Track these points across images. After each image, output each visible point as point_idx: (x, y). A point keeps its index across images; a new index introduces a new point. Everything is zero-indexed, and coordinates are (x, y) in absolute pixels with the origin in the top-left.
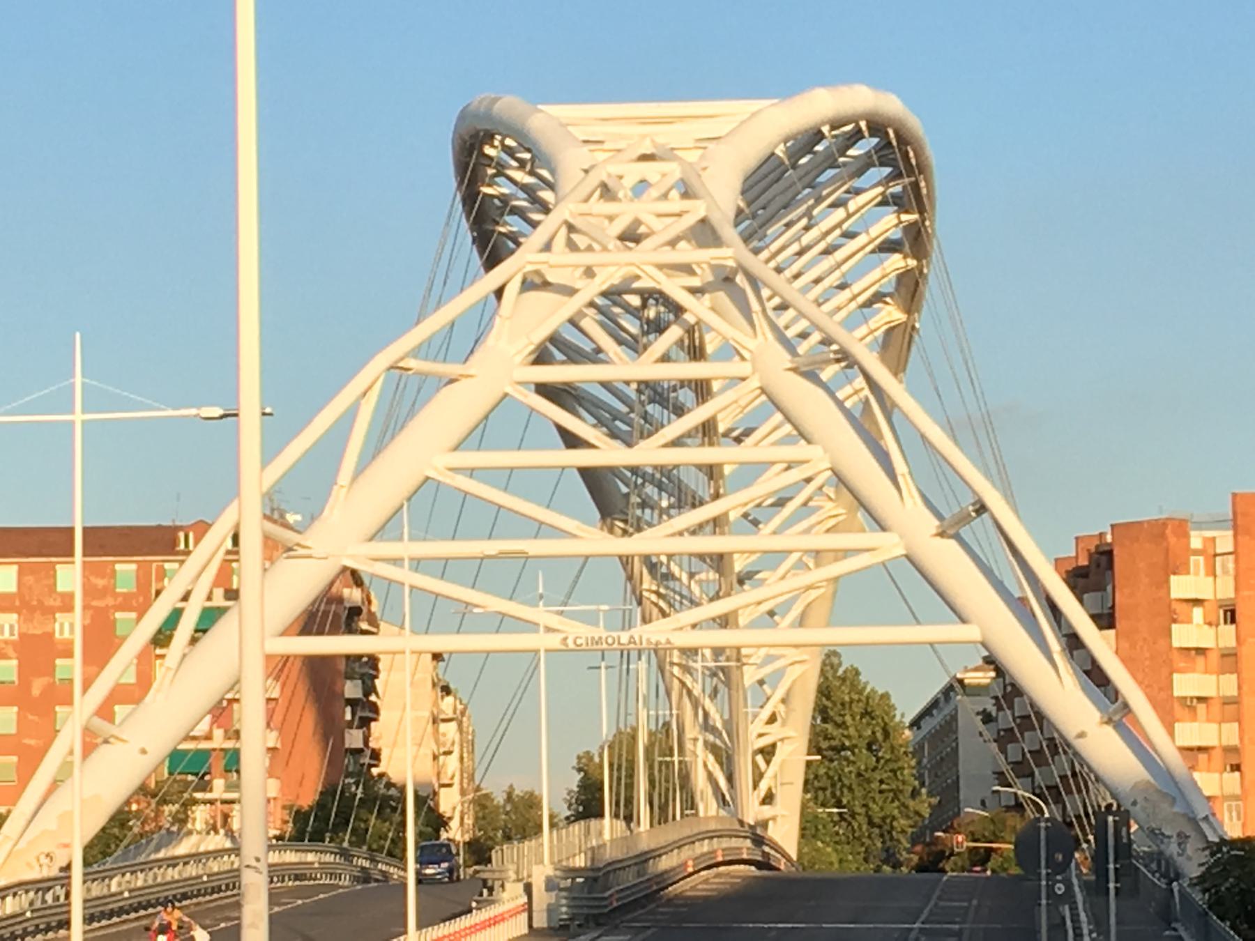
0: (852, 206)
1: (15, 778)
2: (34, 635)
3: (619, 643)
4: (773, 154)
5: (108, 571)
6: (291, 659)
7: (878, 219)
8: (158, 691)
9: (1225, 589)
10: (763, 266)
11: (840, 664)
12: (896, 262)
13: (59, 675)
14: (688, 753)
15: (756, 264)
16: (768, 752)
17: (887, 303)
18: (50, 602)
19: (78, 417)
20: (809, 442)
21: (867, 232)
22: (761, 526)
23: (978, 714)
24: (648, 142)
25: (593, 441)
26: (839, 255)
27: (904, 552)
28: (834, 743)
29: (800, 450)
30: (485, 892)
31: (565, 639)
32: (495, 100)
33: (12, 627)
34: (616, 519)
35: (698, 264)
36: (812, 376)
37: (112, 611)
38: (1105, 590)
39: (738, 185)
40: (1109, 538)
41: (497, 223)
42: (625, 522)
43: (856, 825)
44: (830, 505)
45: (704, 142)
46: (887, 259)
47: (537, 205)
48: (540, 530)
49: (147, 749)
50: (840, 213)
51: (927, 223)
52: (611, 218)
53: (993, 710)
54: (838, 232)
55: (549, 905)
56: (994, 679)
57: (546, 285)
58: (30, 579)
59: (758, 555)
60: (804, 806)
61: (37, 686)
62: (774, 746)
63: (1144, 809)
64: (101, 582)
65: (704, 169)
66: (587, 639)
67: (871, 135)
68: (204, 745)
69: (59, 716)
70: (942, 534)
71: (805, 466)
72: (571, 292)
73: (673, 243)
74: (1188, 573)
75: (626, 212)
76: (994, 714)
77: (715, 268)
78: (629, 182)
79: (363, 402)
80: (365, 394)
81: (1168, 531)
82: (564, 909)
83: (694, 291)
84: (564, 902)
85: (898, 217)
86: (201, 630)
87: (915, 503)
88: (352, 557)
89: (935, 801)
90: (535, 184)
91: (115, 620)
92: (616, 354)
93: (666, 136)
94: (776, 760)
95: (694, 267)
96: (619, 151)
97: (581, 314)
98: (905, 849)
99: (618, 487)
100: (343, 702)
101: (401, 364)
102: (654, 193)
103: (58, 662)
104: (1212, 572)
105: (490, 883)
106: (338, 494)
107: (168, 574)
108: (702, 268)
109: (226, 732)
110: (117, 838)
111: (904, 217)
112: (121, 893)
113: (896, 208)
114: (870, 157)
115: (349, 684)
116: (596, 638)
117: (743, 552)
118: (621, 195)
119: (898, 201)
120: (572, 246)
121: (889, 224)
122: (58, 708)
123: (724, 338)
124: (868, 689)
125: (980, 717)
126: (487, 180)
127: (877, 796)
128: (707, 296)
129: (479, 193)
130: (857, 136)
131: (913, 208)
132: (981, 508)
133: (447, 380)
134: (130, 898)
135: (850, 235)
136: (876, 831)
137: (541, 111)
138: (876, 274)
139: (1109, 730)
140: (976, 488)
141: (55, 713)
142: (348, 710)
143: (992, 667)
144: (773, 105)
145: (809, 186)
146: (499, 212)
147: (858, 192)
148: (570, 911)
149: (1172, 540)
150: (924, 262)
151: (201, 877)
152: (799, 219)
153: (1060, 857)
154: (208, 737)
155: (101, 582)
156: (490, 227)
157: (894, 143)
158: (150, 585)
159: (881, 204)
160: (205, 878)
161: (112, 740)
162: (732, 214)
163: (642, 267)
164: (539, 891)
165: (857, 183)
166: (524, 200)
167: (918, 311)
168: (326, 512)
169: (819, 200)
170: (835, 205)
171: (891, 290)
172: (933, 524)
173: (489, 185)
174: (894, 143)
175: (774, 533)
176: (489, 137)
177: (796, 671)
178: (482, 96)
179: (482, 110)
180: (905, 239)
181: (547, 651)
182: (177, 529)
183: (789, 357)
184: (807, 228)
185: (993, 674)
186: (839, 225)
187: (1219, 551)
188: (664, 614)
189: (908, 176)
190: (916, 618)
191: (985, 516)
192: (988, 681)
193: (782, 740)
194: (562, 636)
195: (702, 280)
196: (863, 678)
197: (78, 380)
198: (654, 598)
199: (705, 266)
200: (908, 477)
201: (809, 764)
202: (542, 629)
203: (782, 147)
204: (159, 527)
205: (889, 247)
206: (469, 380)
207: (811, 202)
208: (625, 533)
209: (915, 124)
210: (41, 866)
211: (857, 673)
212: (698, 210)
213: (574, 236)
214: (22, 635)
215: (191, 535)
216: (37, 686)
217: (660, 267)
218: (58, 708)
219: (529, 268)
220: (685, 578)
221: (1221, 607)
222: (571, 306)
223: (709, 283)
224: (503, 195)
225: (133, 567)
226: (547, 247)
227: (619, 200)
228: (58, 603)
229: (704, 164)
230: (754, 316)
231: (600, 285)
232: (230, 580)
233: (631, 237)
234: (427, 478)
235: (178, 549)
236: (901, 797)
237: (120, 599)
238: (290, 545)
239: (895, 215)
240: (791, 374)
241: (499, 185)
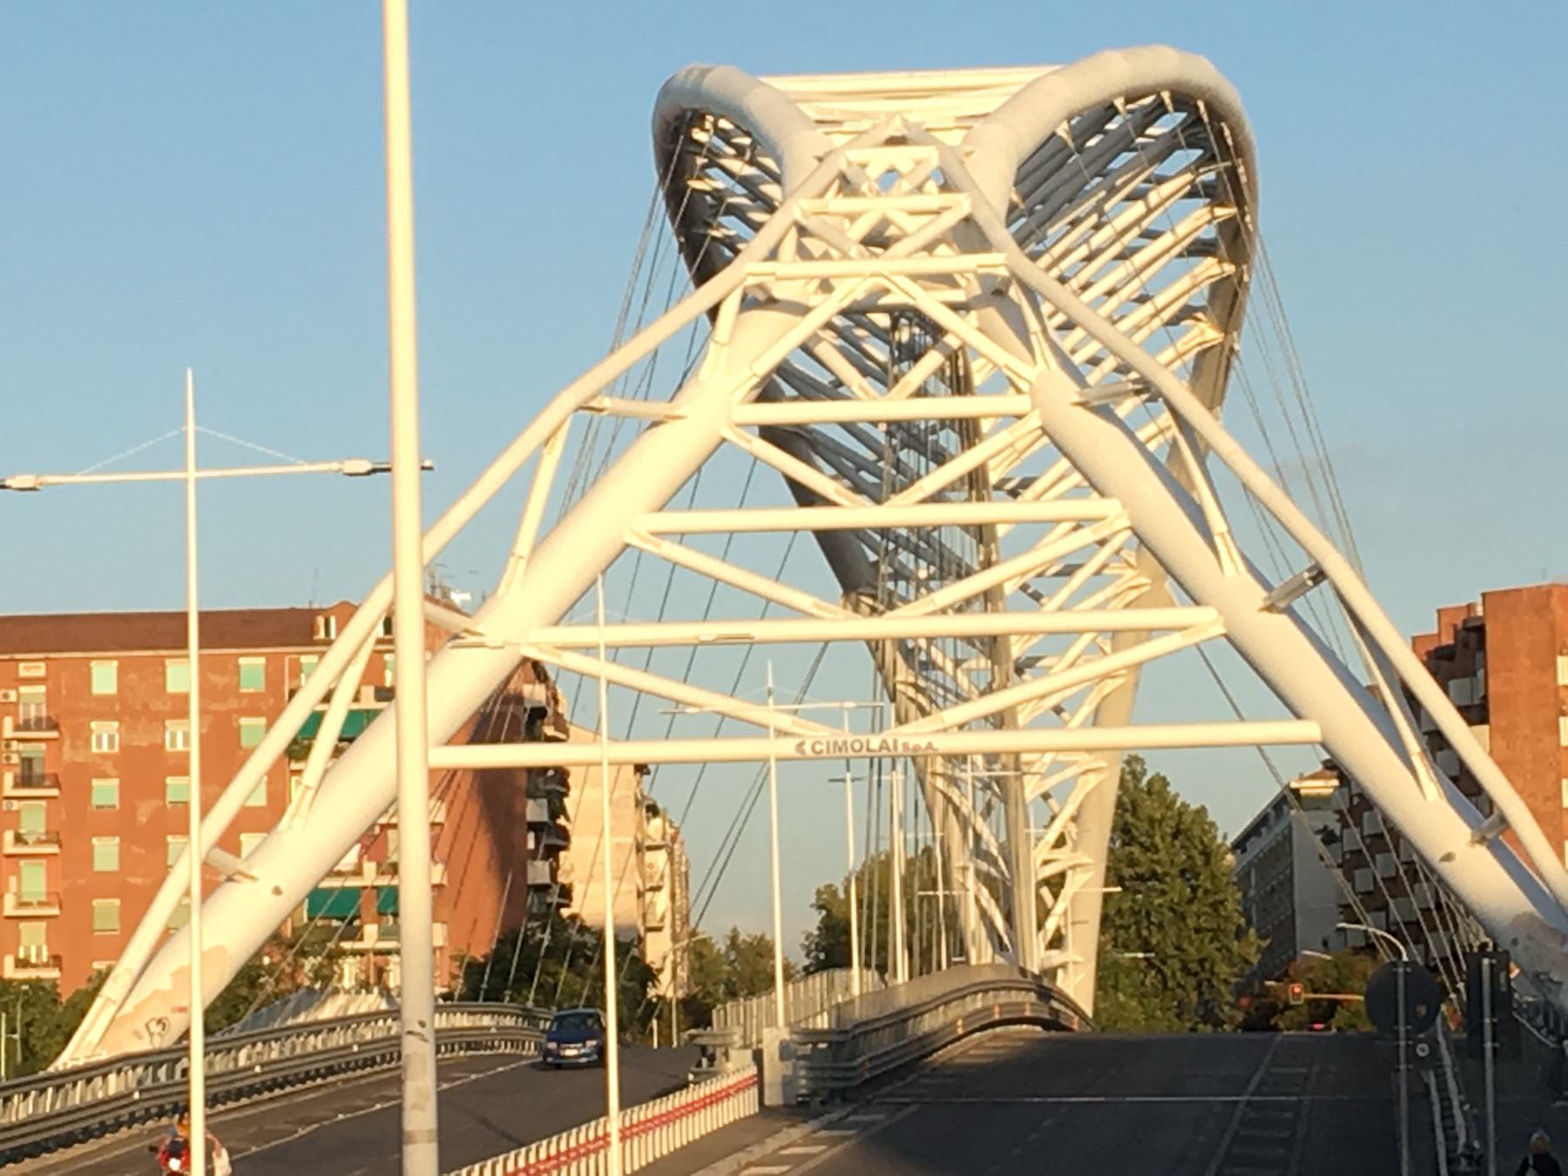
0: (1154, 198)
1: (117, 926)
2: (139, 748)
4: (1054, 134)
5: (230, 667)
6: (459, 774)
7: (1185, 215)
8: (295, 815)
10: (1043, 274)
11: (1144, 772)
12: (1210, 268)
13: (170, 797)
14: (955, 885)
15: (1034, 273)
16: (1056, 883)
17: (1198, 320)
18: (156, 706)
19: (192, 474)
20: (1102, 494)
21: (1173, 231)
22: (1043, 601)
23: (1318, 832)
24: (897, 122)
25: (833, 496)
26: (1139, 259)
27: (1223, 631)
28: (1138, 870)
29: (1091, 505)
30: (705, 1061)
31: (801, 745)
32: (704, 73)
33: (111, 738)
34: (862, 594)
35: (961, 273)
36: (1105, 412)
37: (235, 716)
38: (1474, 674)
39: (1010, 174)
40: (1480, 611)
41: (709, 226)
42: (874, 597)
43: (1169, 973)
44: (1129, 573)
45: (967, 122)
46: (1196, 265)
47: (759, 203)
48: (768, 608)
49: (283, 887)
50: (1138, 208)
51: (1248, 219)
52: (852, 217)
53: (1336, 828)
54: (1136, 231)
55: (784, 1077)
56: (1335, 788)
57: (771, 302)
58: (133, 676)
59: (1041, 637)
60: (1101, 952)
62: (1062, 875)
63: (1526, 948)
64: (220, 680)
65: (968, 154)
66: (828, 743)
67: (1176, 110)
68: (353, 882)
69: (171, 848)
70: (1270, 608)
71: (1097, 525)
72: (803, 310)
73: (929, 248)
75: (870, 210)
76: (1338, 832)
77: (984, 279)
78: (874, 171)
79: (545, 451)
80: (547, 442)
81: (1554, 601)
82: (803, 1082)
83: (956, 307)
84: (803, 1072)
85: (1212, 212)
86: (347, 738)
87: (1237, 569)
88: (535, 645)
89: (1265, 944)
90: (758, 177)
91: (239, 727)
92: (861, 388)
93: (920, 112)
94: (1067, 892)
95: (958, 278)
96: (860, 133)
97: (815, 338)
98: (1228, 1003)
99: (866, 558)
100: (526, 827)
101: (594, 404)
102: (906, 185)
103: (169, 780)
105: (710, 1051)
106: (516, 568)
107: (304, 668)
108: (968, 280)
109: (379, 865)
110: (245, 999)
111: (1219, 211)
112: (251, 1068)
113: (1208, 200)
114: (1176, 136)
115: (531, 803)
116: (840, 743)
117: (1021, 633)
118: (864, 188)
119: (1211, 191)
120: (803, 253)
121: (1199, 220)
122: (170, 839)
123: (995, 365)
124: (1178, 804)
125: (1319, 837)
126: (696, 173)
127: (1194, 936)
128: (973, 314)
129: (687, 186)
130: (1158, 110)
131: (1229, 201)
132: (1319, 575)
133: (649, 423)
134: (263, 1073)
135: (1151, 235)
136: (1192, 981)
137: (764, 84)
138: (1183, 284)
139: (1482, 852)
140: (1314, 553)
141: (166, 844)
142: (531, 837)
143: (1335, 773)
144: (1054, 73)
145: (1101, 173)
146: (709, 212)
147: (1160, 180)
148: (812, 1085)
150: (1245, 267)
151: (349, 1047)
152: (1088, 215)
153: (1422, 1010)
154: (358, 872)
155: (220, 680)
156: (701, 231)
157: (1206, 118)
158: (283, 683)
159: (1193, 194)
160: (355, 1048)
161: (237, 877)
162: (1003, 209)
163: (894, 278)
164: (772, 1059)
165: (1158, 170)
166: (744, 196)
167: (1238, 328)
168: (500, 592)
169: (1113, 191)
170: (1132, 198)
171: (1204, 303)
172: (1260, 595)
173: (699, 178)
174: (1206, 118)
175: (1060, 609)
176: (698, 118)
177: (1093, 780)
178: (688, 67)
179: (688, 86)
180: (1220, 241)
181: (778, 760)
182: (312, 614)
183: (1076, 388)
184: (1097, 227)
185: (1335, 782)
186: (1138, 222)
188: (924, 712)
189: (1223, 160)
190: (1239, 715)
191: (1324, 584)
192: (1331, 791)
193: (1073, 868)
194: (798, 741)
195: (968, 293)
196: (1172, 790)
197: (191, 427)
198: (911, 692)
199: (971, 276)
200: (1228, 537)
201: (1107, 897)
202: (772, 732)
203: (1065, 125)
204: (292, 610)
205: (1200, 249)
206: (678, 422)
207: (1102, 194)
208: (873, 610)
209: (1232, 94)
210: (151, 1034)
211: (1164, 782)
212: (961, 205)
213: (806, 241)
214: (123, 748)
215: (333, 621)
217: (915, 278)
218: (170, 839)
219: (751, 281)
220: (949, 666)
222: (805, 327)
223: (975, 298)
224: (717, 190)
225: (262, 660)
226: (773, 255)
227: (864, 195)
228: (168, 707)
229: (968, 148)
230: (1033, 338)
231: (840, 301)
232: (382, 676)
233: (877, 240)
234: (627, 546)
235: (316, 638)
236: (1221, 937)
237: (245, 702)
238: (455, 631)
239: (1206, 210)
240: (1080, 410)
241: (710, 177)
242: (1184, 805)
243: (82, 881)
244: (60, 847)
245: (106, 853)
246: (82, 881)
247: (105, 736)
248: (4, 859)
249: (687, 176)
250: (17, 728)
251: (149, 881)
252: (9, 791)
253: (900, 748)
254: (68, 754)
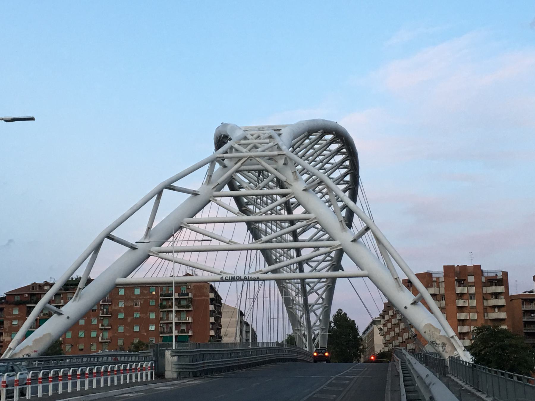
2: (129, 306)
18: (133, 298)
58: (127, 291)
61: (129, 320)
74: (432, 287)
100: (209, 323)
104: (438, 286)
142: (211, 325)
155: (146, 292)
187: (440, 281)
216: (129, 320)
221: (441, 296)
228: (135, 297)
242: (350, 320)
243: (116, 334)
244: (111, 327)
245: (121, 329)
246: (116, 334)
247: (121, 305)
248: (99, 330)
250: (102, 302)
251: (130, 334)
252: (101, 315)
254: (113, 308)
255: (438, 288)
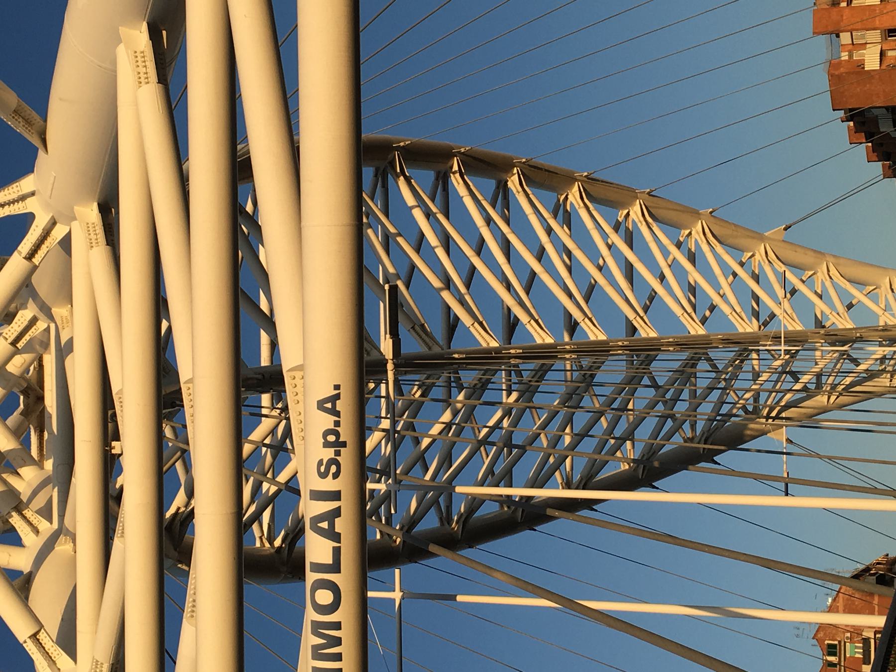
3: (335, 567)
9: (874, 36)
74: (864, 60)
81: (837, 73)
111: (456, 168)
149: (842, 70)
249: (393, 545)
253: (328, 484)
255: (868, 46)
